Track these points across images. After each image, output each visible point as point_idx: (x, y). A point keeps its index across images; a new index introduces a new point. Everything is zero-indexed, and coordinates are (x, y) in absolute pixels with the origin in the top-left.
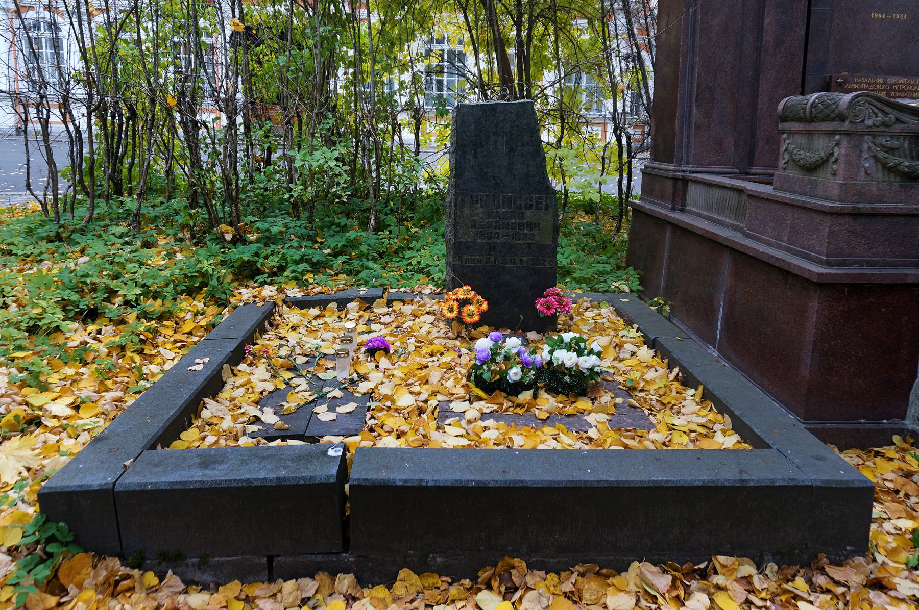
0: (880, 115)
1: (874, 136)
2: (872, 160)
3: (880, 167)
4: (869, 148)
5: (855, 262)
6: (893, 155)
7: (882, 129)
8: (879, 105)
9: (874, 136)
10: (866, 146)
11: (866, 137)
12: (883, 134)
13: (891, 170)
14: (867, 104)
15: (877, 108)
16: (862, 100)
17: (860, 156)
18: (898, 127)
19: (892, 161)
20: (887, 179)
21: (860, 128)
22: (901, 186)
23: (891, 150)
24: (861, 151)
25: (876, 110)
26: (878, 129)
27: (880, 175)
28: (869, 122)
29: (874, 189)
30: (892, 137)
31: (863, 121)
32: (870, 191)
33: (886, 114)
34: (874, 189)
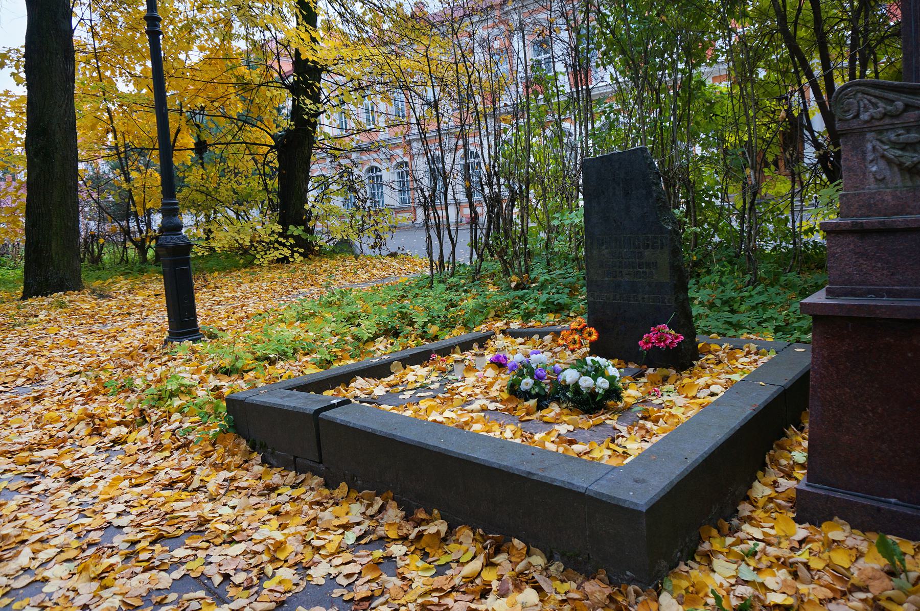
0: (881, 104)
2: (882, 164)
3: (896, 169)
4: (874, 147)
5: (869, 292)
7: (887, 121)
8: (877, 92)
9: (880, 132)
10: (869, 146)
11: (869, 136)
14: (860, 95)
15: (876, 97)
16: (851, 91)
17: (864, 159)
20: (909, 184)
21: (854, 124)
23: (904, 147)
24: (864, 153)
25: (874, 100)
26: (881, 123)
27: (898, 179)
28: (865, 116)
29: (889, 198)
30: (908, 130)
31: (857, 116)
32: (884, 201)
33: (891, 102)
34: (889, 198)
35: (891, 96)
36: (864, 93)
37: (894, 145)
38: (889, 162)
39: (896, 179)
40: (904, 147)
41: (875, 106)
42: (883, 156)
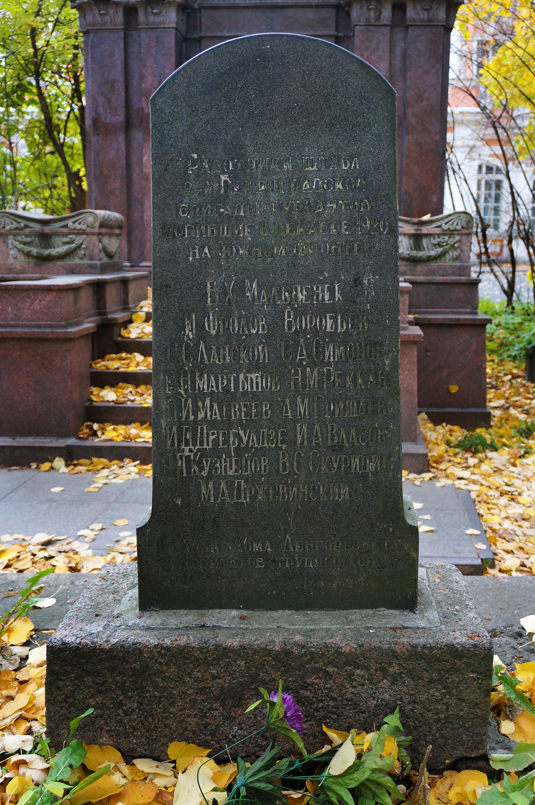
1: (15, 236)
2: (16, 250)
6: (29, 246)
7: (17, 231)
8: (13, 218)
10: (10, 242)
11: (10, 237)
12: (20, 235)
13: (28, 255)
17: (8, 247)
18: (27, 230)
19: (27, 249)
22: (35, 264)
23: (25, 244)
24: (8, 244)
25: (12, 221)
28: (8, 228)
30: (27, 236)
31: (4, 227)
33: (19, 223)
35: (19, 220)
36: (7, 217)
37: (21, 242)
38: (19, 250)
39: (22, 258)
40: (25, 244)
41: (12, 223)
42: (16, 247)
